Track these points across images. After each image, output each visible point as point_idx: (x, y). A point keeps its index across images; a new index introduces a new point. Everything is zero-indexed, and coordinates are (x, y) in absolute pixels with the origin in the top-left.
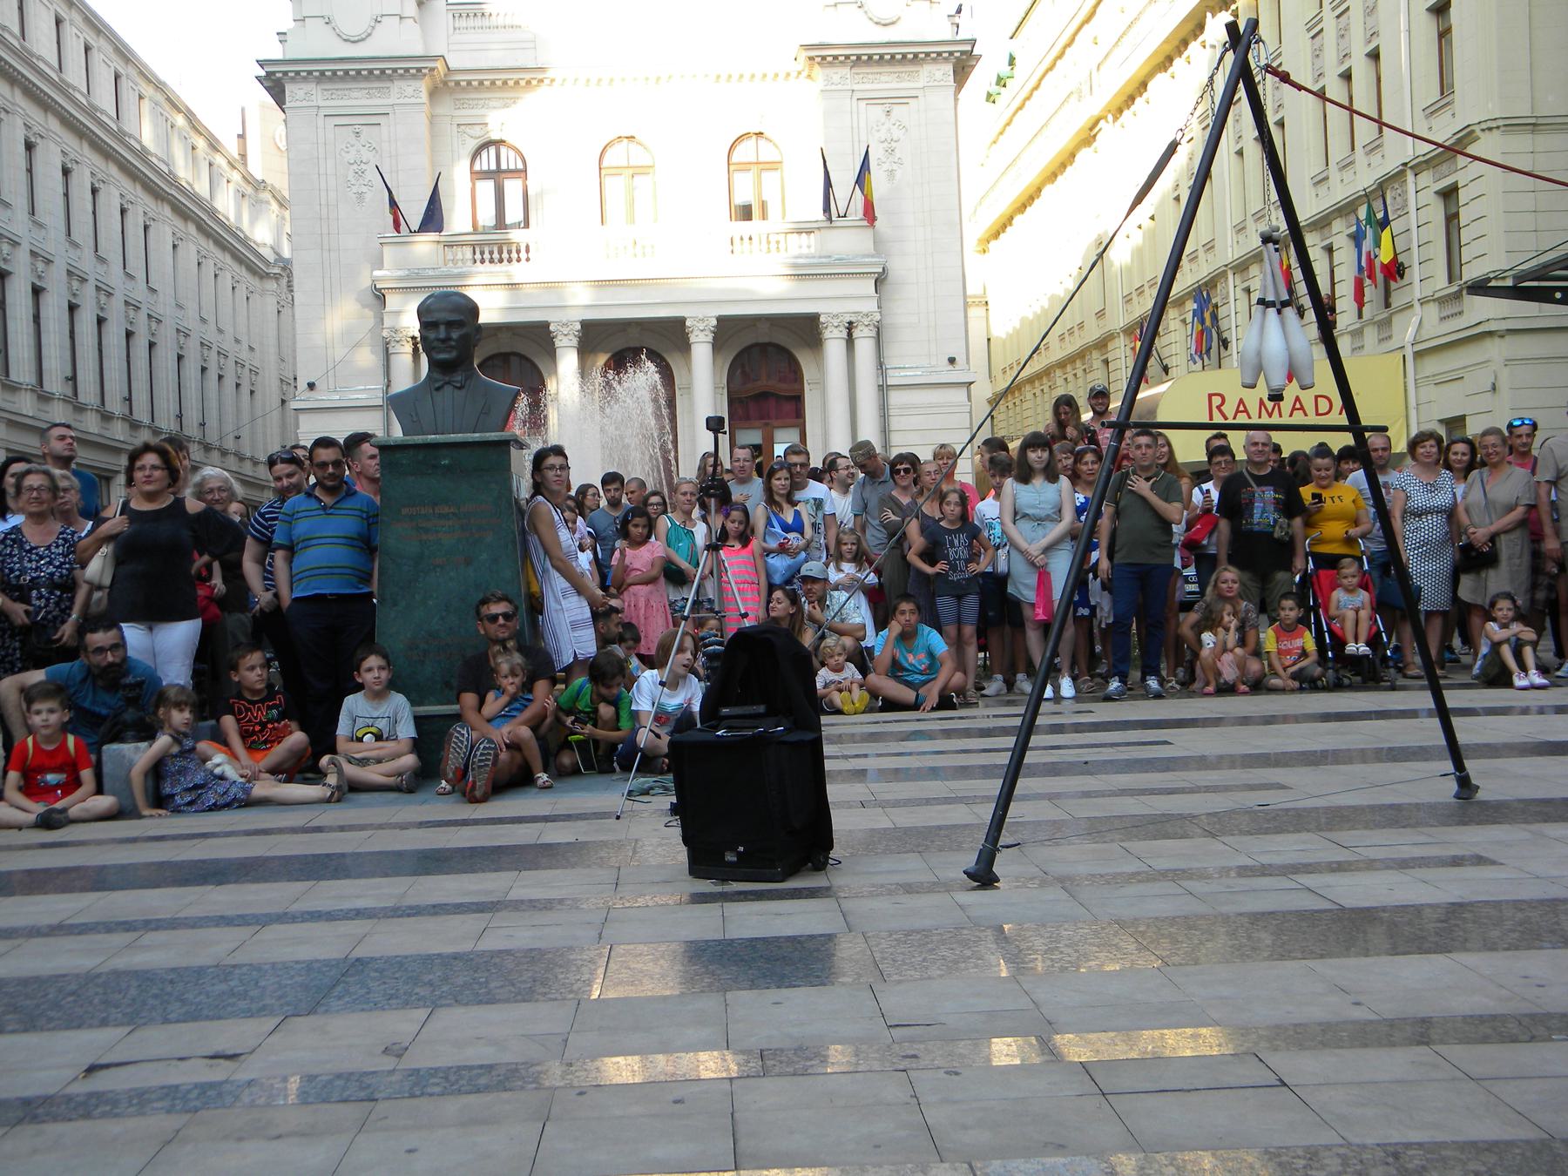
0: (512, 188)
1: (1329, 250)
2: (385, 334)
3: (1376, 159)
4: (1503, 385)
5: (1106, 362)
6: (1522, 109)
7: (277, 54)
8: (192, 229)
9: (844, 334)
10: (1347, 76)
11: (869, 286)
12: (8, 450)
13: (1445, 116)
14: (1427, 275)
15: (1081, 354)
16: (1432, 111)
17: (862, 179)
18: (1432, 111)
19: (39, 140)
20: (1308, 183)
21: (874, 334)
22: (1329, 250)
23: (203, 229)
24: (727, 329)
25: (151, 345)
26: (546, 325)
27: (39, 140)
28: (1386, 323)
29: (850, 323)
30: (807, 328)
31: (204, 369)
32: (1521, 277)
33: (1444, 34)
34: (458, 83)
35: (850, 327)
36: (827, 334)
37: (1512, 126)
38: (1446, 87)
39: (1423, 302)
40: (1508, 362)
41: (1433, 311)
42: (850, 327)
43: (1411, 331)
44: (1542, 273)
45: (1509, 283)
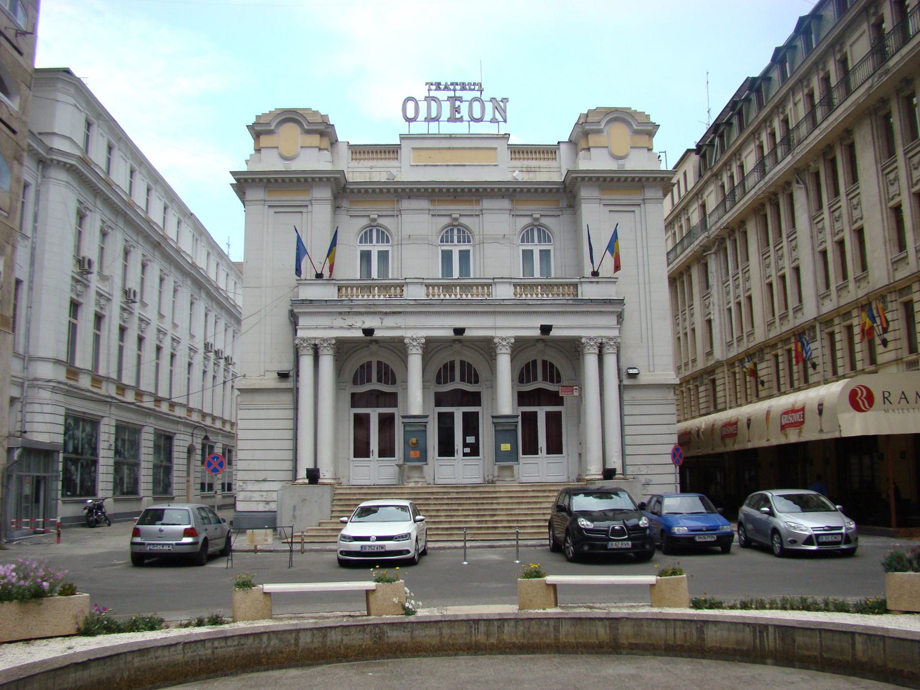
2: (297, 342)
7: (244, 168)
8: (203, 295)
9: (597, 351)
11: (613, 321)
12: (67, 409)
17: (612, 247)
19: (110, 231)
21: (615, 351)
23: (209, 294)
24: (519, 346)
25: (173, 356)
26: (401, 340)
27: (110, 231)
29: (601, 344)
30: (573, 349)
31: (204, 372)
34: (352, 191)
35: (601, 347)
36: (586, 351)
42: (601, 347)
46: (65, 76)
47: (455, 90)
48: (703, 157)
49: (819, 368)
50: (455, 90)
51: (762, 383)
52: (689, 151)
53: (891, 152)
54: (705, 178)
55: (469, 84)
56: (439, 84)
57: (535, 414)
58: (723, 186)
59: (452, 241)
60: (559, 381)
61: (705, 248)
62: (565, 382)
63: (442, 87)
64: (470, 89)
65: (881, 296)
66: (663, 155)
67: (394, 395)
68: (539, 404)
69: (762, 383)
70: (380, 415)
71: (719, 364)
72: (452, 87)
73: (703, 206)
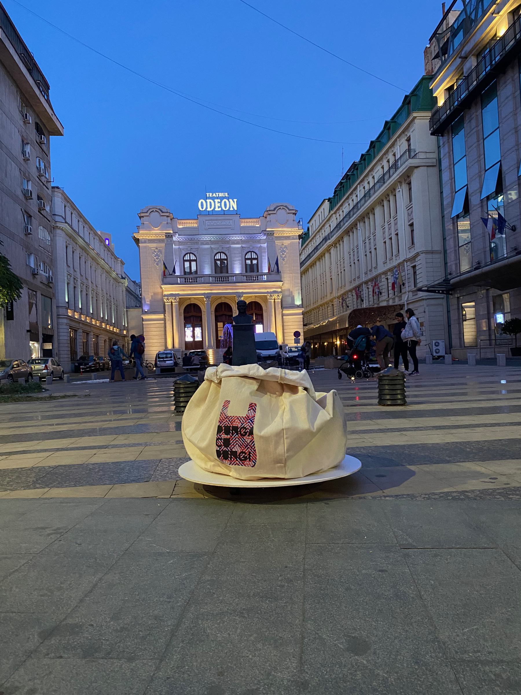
0: (193, 264)
1: (387, 279)
3: (398, 258)
4: (427, 310)
5: (333, 305)
6: (430, 249)
10: (391, 239)
13: (413, 249)
14: (409, 286)
15: (327, 303)
16: (410, 248)
18: (410, 248)
20: (382, 263)
22: (387, 279)
28: (401, 296)
32: (428, 288)
33: (412, 231)
37: (427, 252)
38: (413, 243)
39: (409, 292)
40: (428, 305)
41: (411, 293)
43: (406, 299)
44: (433, 287)
45: (426, 289)
46: (56, 190)
48: (331, 203)
49: (364, 301)
51: (348, 307)
52: (325, 200)
54: (330, 214)
61: (329, 246)
65: (380, 275)
66: (301, 220)
69: (348, 307)
71: (335, 298)
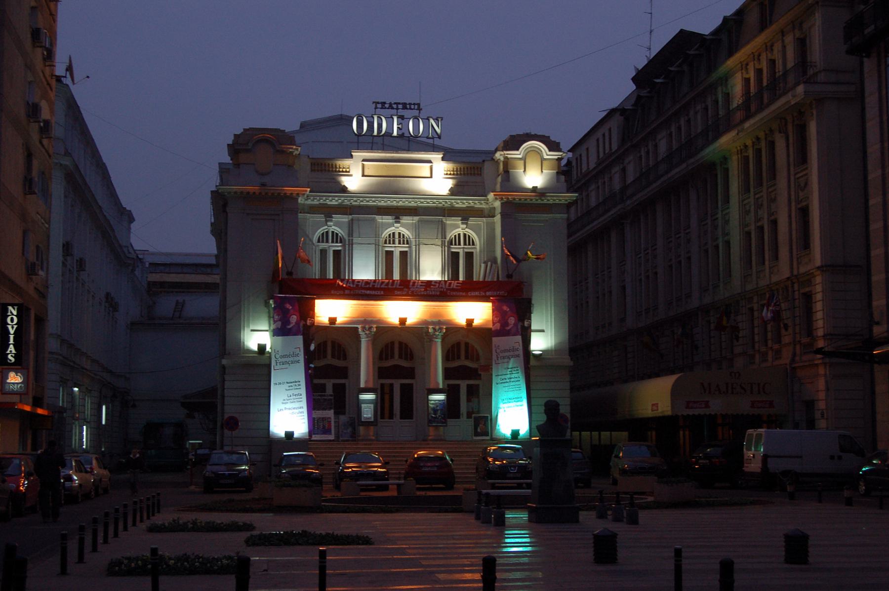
47: (397, 109)
50: (397, 109)
53: (748, 190)
55: (410, 104)
56: (385, 103)
57: (458, 387)
58: (641, 157)
59: (394, 243)
60: (478, 359)
62: (482, 362)
63: (387, 106)
64: (411, 109)
67: (346, 368)
68: (463, 379)
70: (334, 385)
72: (395, 106)
73: (624, 170)
